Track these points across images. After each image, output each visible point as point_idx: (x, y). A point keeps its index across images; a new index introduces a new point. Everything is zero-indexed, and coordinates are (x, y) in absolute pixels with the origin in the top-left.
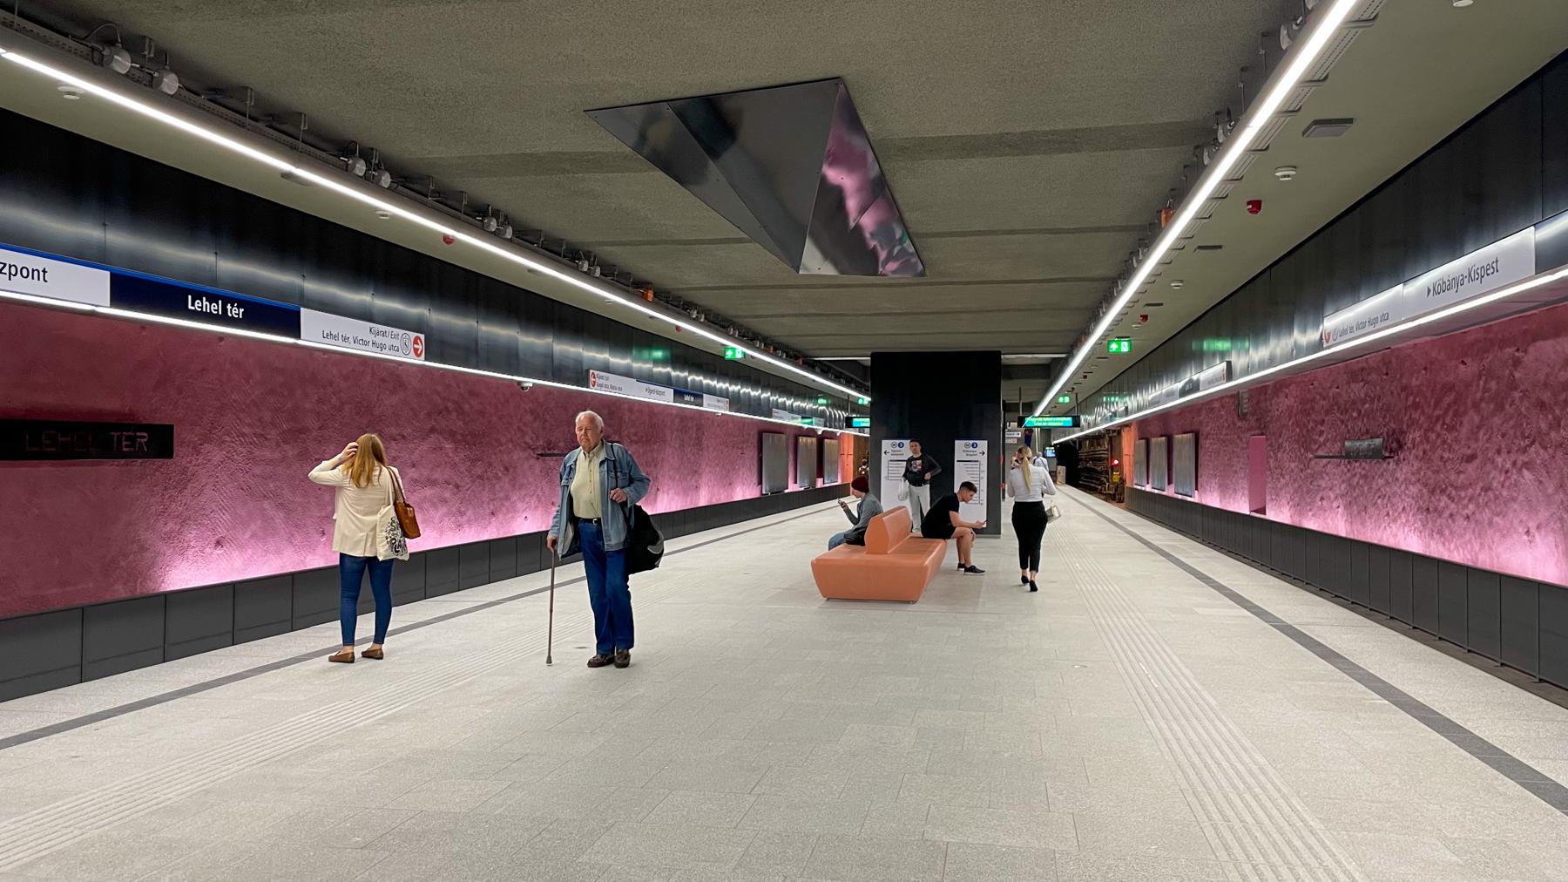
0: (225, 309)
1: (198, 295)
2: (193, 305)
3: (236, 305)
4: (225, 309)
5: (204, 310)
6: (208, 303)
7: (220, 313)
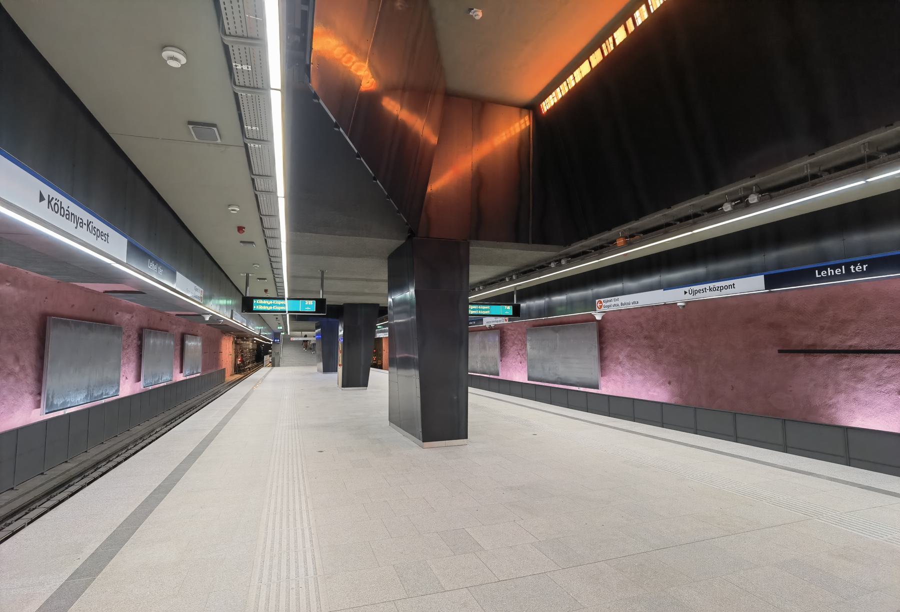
0: (848, 269)
1: (820, 269)
2: (819, 274)
3: (859, 264)
4: (848, 269)
5: (829, 274)
6: (832, 271)
7: (844, 272)
